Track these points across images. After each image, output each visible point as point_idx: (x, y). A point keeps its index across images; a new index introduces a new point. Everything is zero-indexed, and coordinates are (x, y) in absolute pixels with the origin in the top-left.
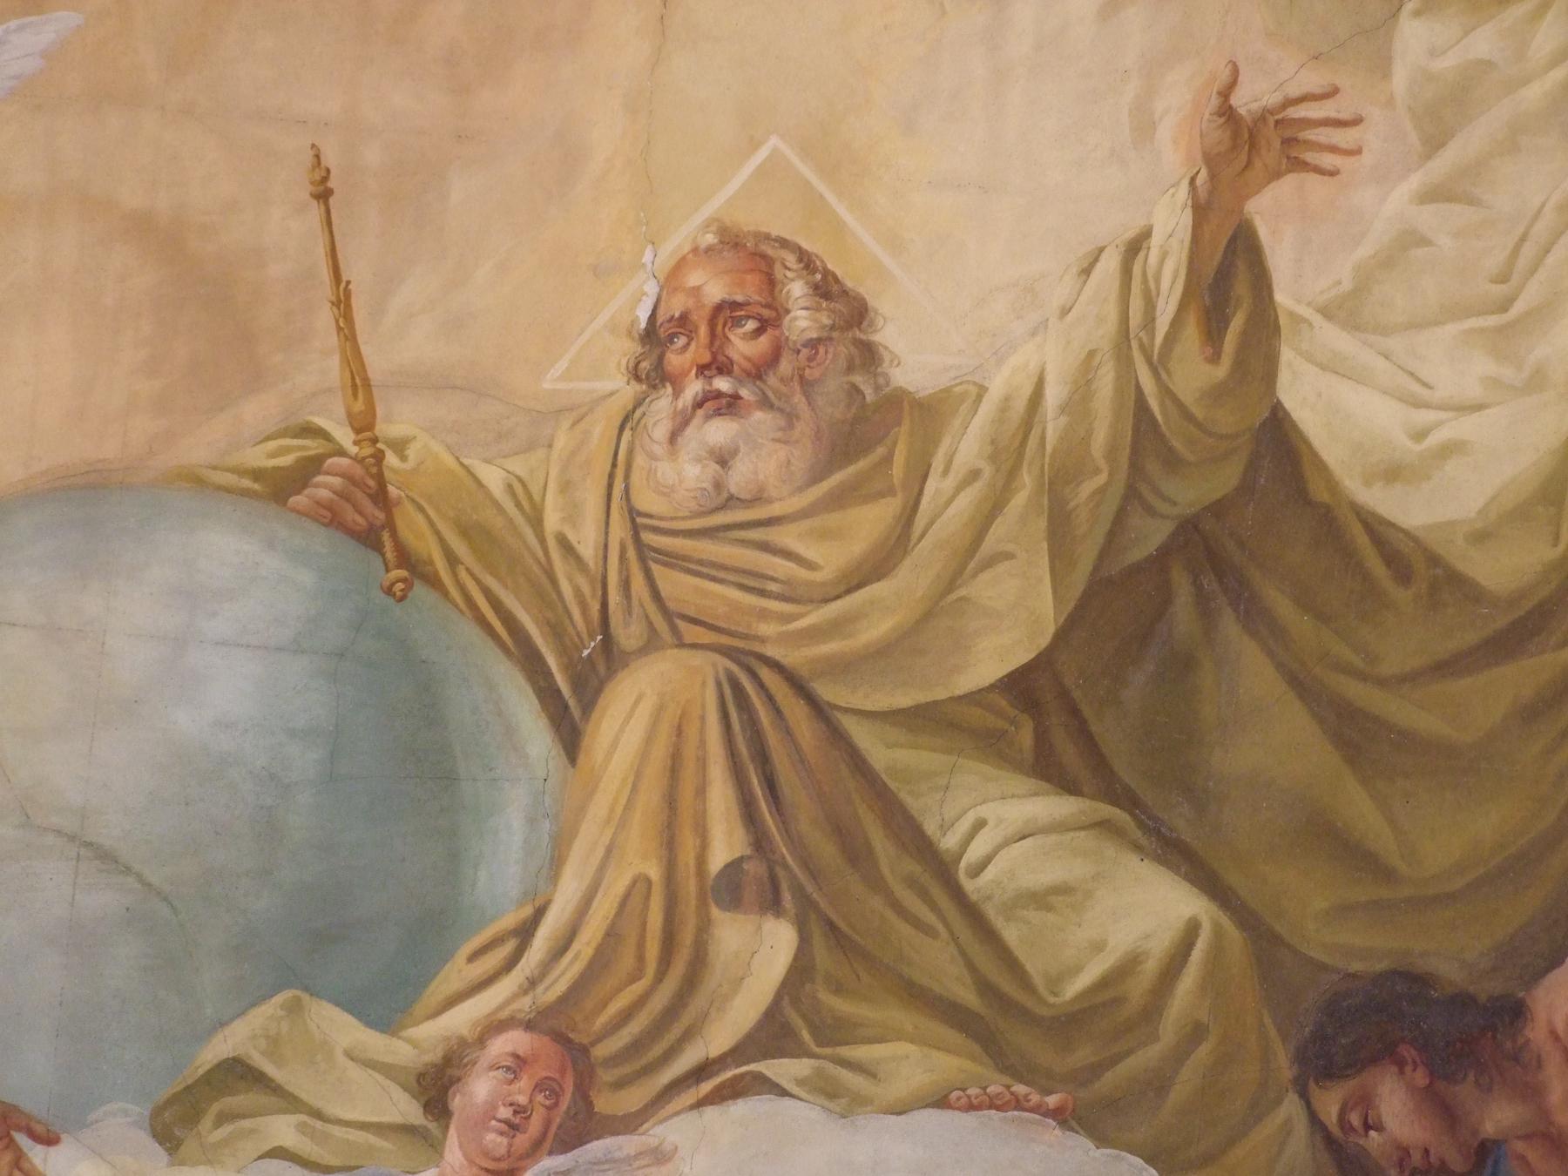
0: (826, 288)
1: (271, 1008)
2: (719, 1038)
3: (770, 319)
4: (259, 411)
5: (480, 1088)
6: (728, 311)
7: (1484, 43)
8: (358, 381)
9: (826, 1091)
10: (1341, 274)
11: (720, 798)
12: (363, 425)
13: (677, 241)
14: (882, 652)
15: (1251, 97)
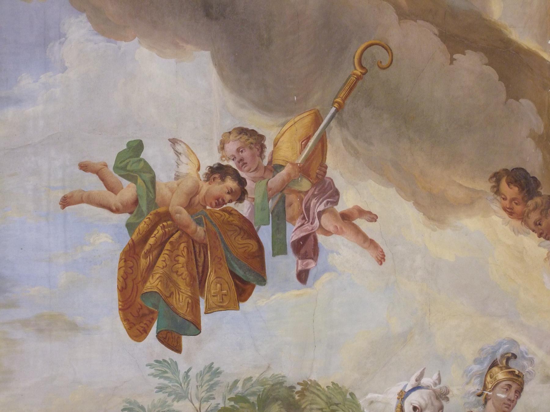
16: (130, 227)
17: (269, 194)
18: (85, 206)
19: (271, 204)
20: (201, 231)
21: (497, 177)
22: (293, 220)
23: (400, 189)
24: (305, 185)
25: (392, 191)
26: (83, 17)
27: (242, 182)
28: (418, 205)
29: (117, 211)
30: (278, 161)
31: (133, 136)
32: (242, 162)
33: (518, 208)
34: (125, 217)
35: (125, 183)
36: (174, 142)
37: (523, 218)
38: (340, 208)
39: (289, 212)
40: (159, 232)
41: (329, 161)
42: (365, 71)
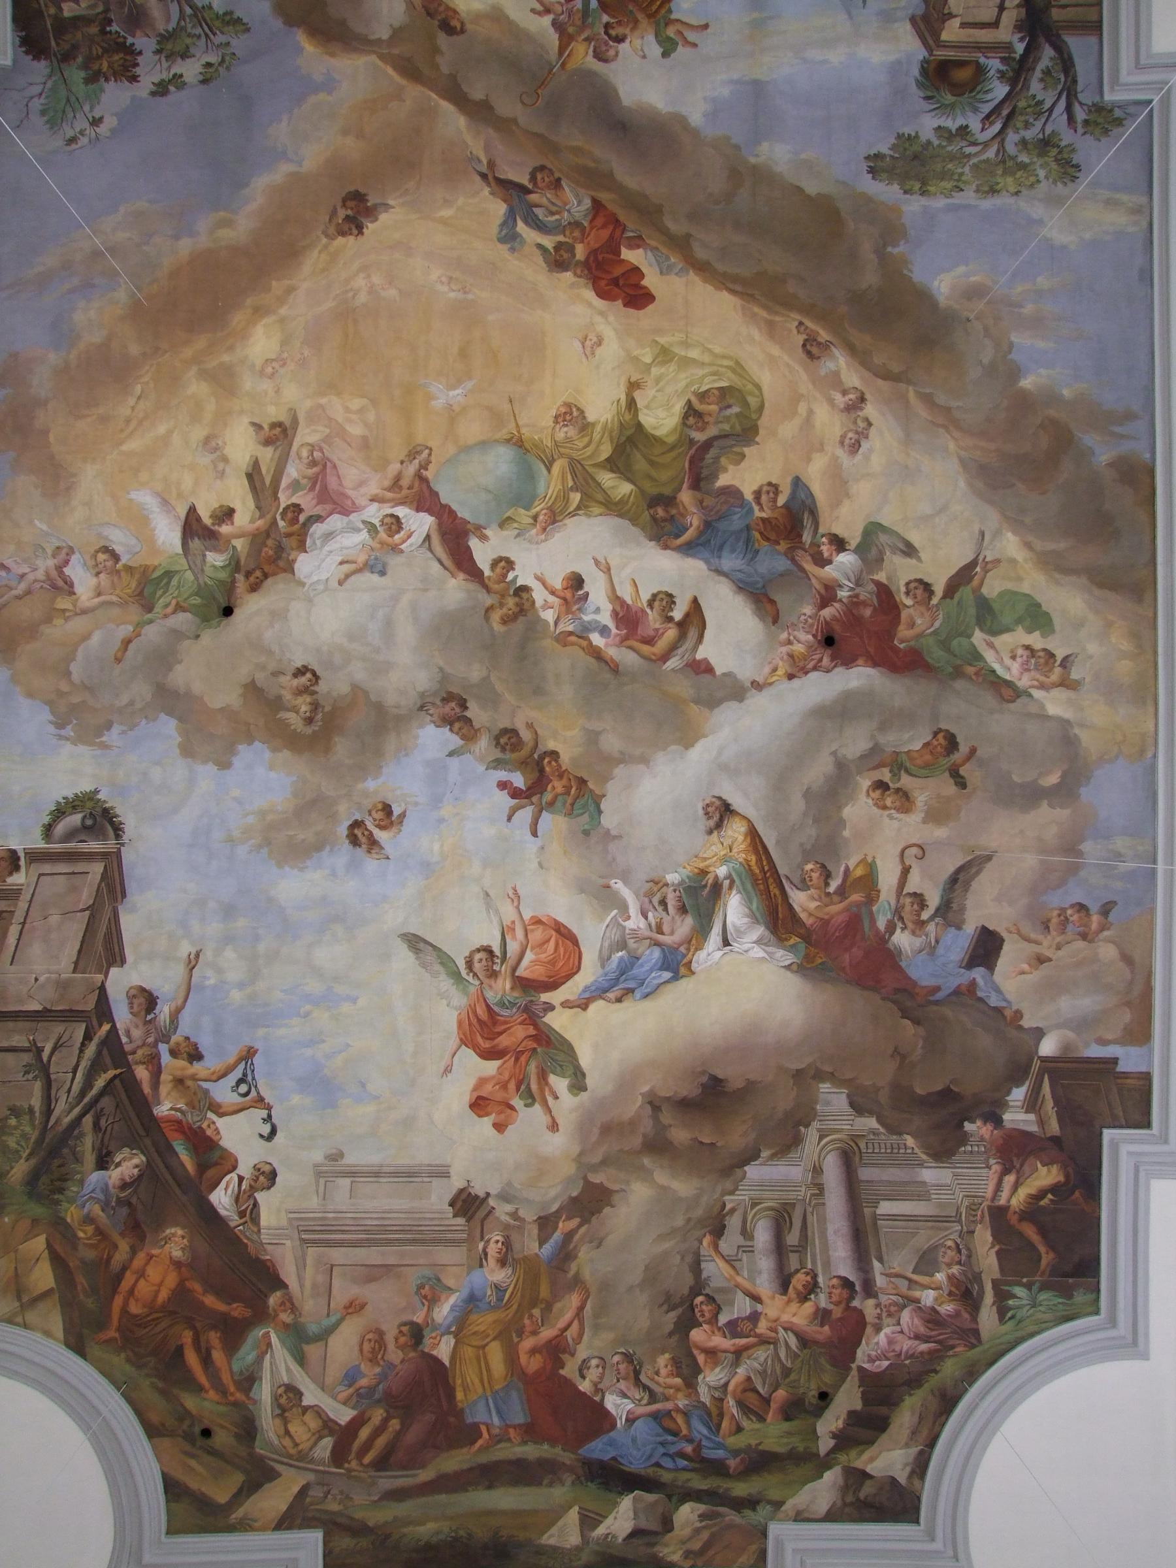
0: (578, 409)
1: (512, 510)
2: (571, 509)
3: (571, 414)
4: (505, 431)
5: (541, 518)
6: (565, 413)
7: (663, 370)
8: (517, 425)
9: (586, 515)
10: (646, 402)
11: (569, 477)
12: (519, 432)
13: (559, 403)
14: (590, 457)
15: (632, 380)
16: (670, 11)
17: (592, 25)
18: (696, 24)
19: (590, 20)
20: (631, 7)
21: (463, 31)
22: (578, 10)
23: (517, 26)
24: (571, 30)
25: (522, 25)
26: (693, 124)
27: (606, 33)
28: (508, 17)
29: (677, 20)
30: (586, 44)
31: (667, 61)
32: (606, 44)
33: (451, 13)
34: (673, 17)
35: (672, 35)
36: (644, 57)
37: (448, 8)
38: (551, 17)
39: (580, 15)
40: (654, 8)
41: (557, 43)
42: (536, 91)
